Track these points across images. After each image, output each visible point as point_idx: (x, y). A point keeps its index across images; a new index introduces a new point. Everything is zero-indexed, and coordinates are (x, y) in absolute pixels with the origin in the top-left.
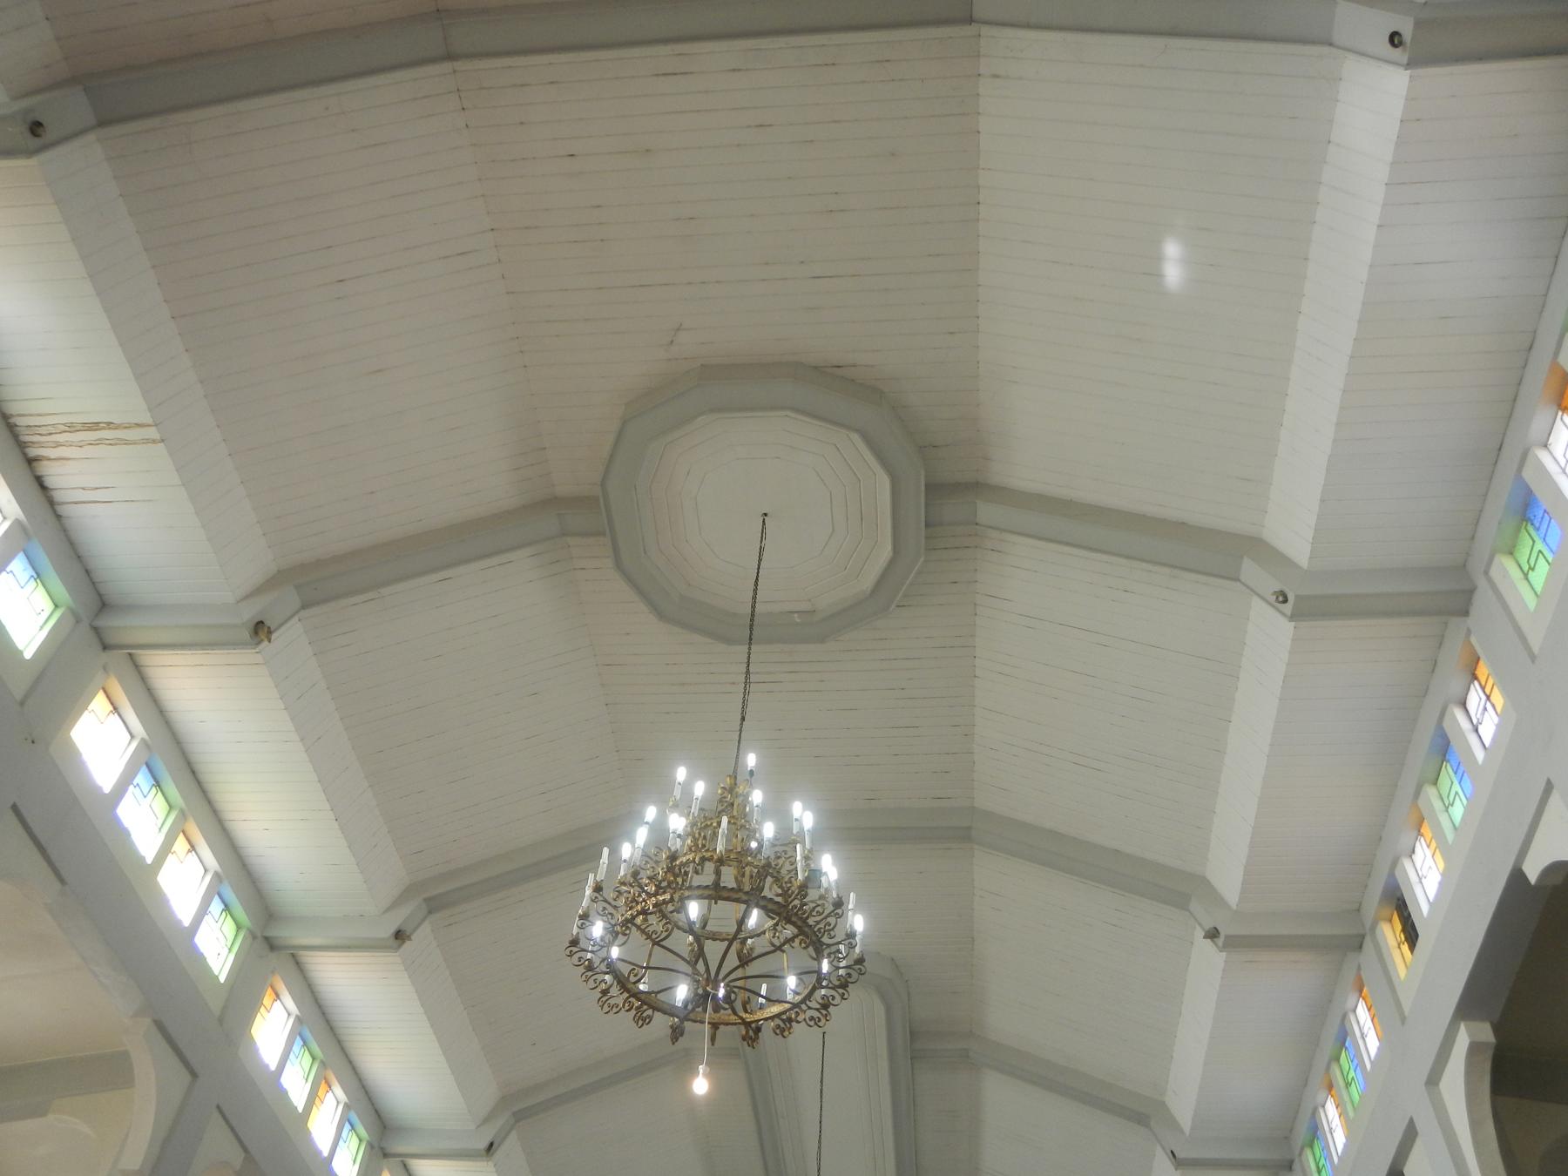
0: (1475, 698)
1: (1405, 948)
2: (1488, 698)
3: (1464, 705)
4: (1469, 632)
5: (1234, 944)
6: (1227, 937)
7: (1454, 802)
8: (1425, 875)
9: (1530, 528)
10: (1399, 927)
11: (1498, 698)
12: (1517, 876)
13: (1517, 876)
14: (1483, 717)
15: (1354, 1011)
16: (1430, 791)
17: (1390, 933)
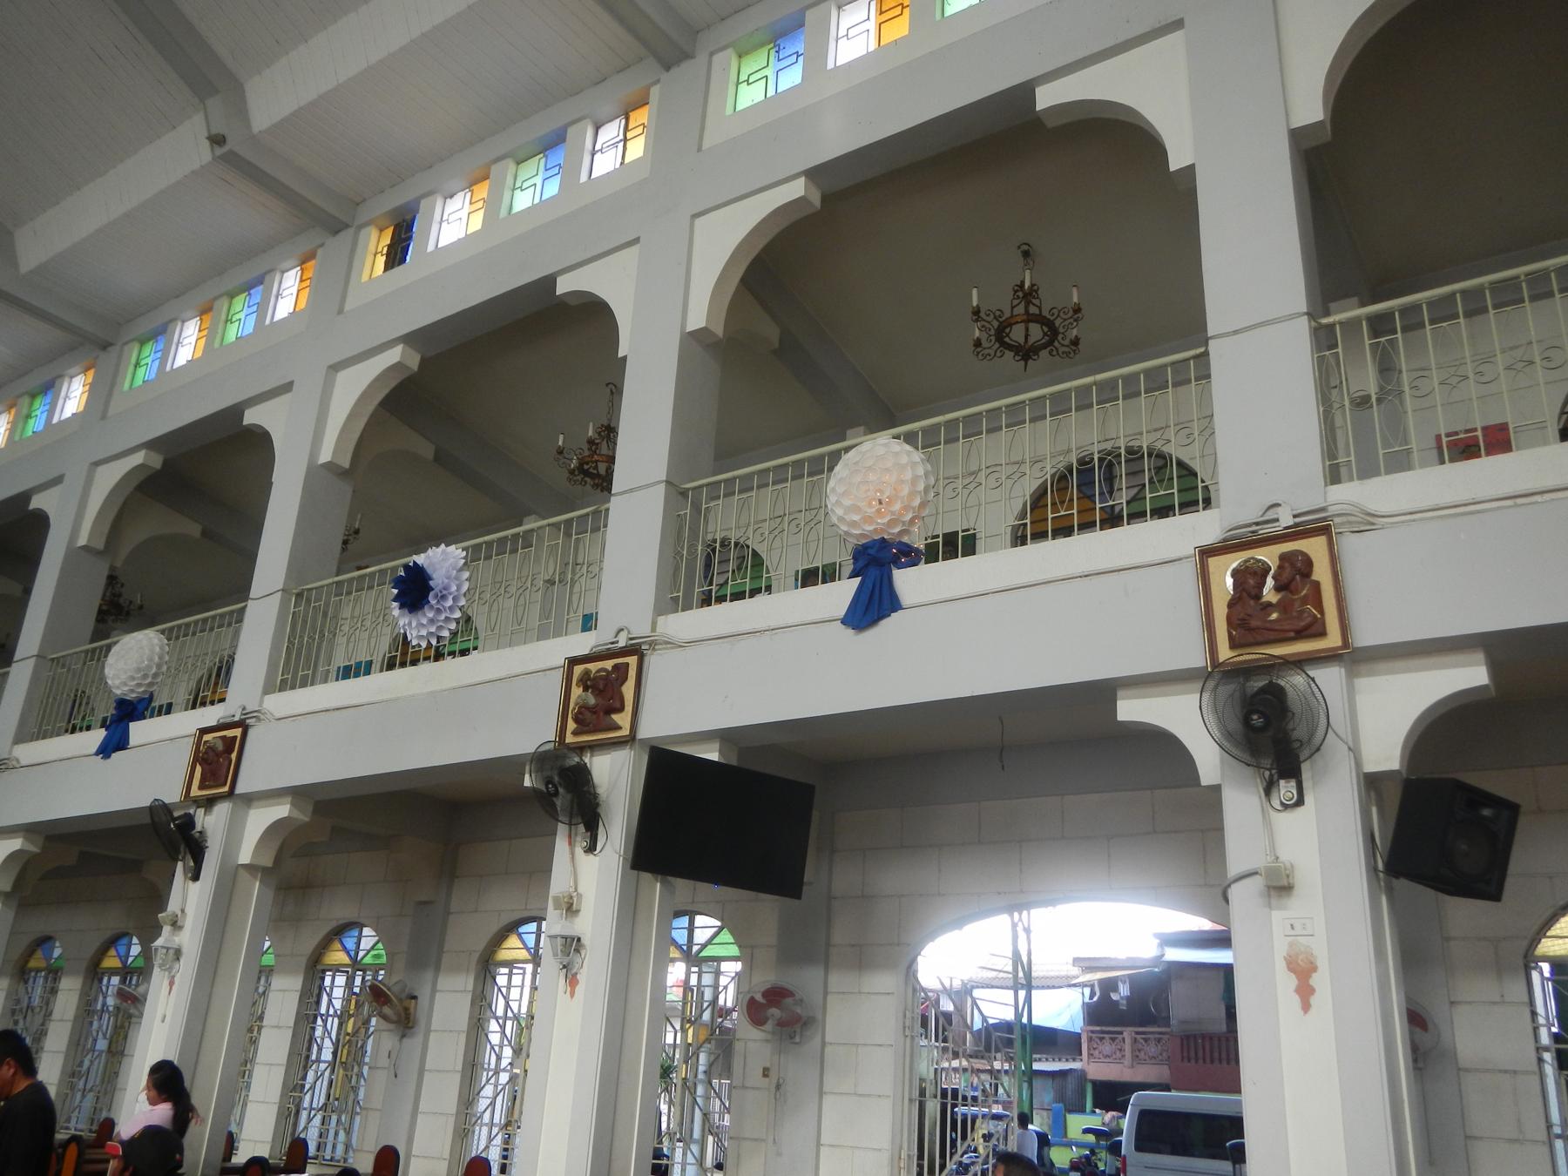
0: (611, 131)
1: (381, 260)
2: (625, 140)
3: (597, 129)
4: (658, 81)
5: (234, 162)
6: (231, 152)
7: (532, 189)
8: (454, 221)
9: (773, 53)
10: (387, 239)
11: (636, 149)
12: (549, 282)
13: (549, 282)
14: (614, 150)
15: (283, 272)
16: (512, 166)
17: (378, 242)
